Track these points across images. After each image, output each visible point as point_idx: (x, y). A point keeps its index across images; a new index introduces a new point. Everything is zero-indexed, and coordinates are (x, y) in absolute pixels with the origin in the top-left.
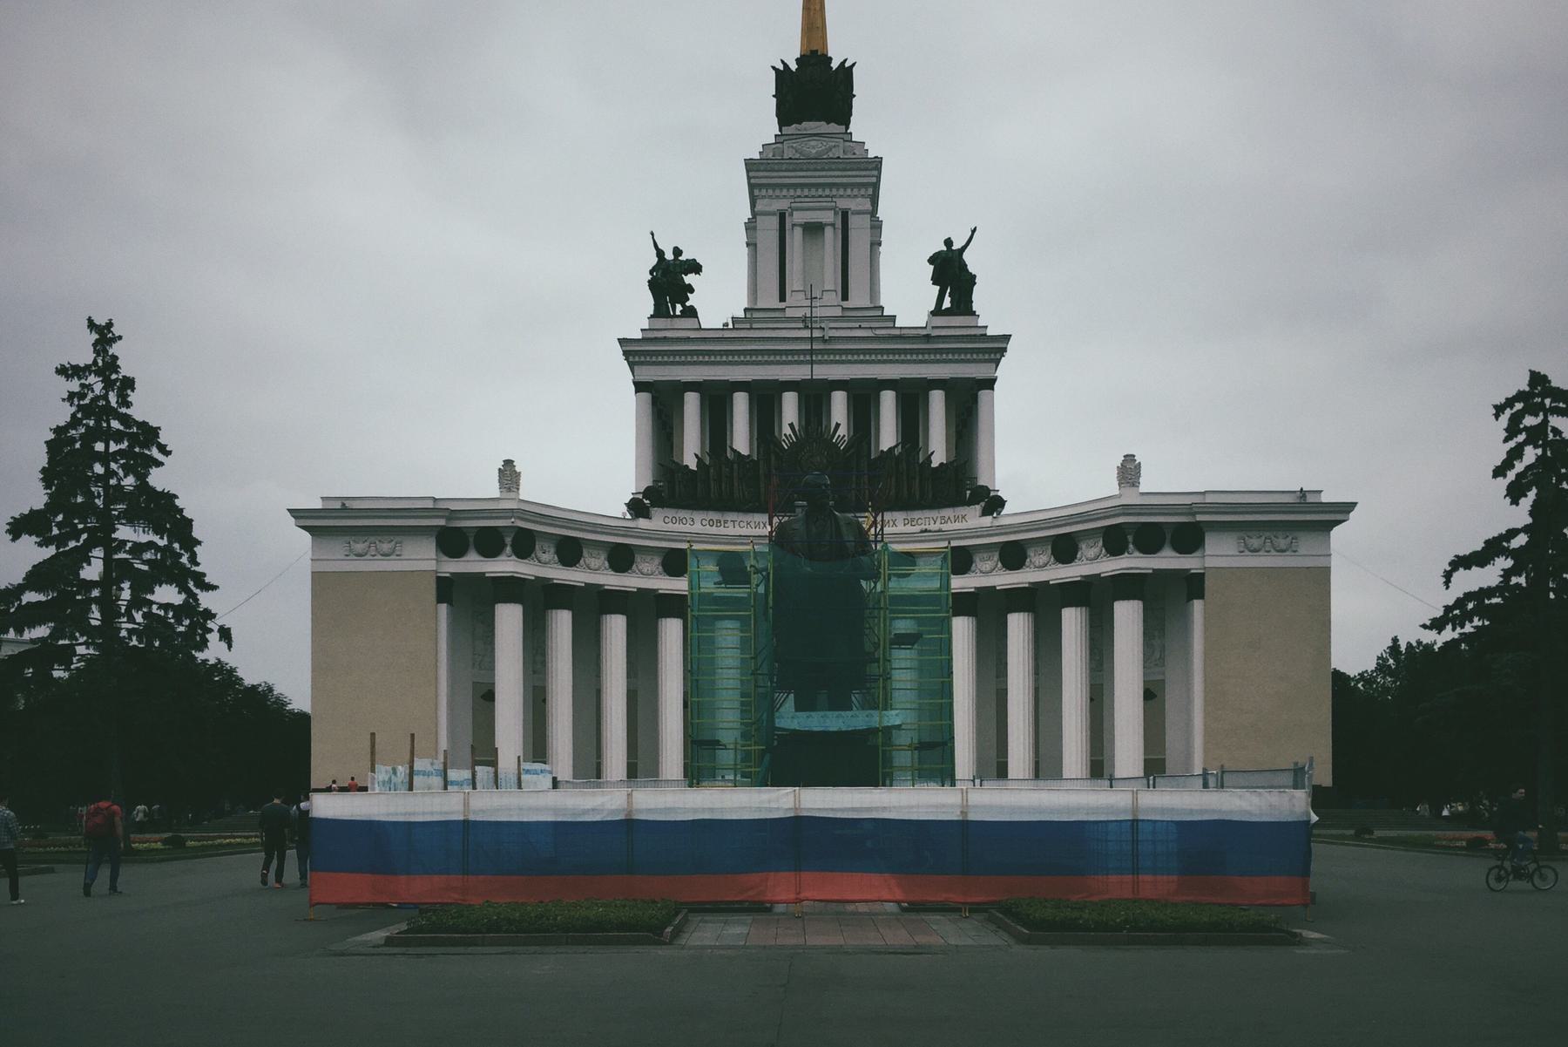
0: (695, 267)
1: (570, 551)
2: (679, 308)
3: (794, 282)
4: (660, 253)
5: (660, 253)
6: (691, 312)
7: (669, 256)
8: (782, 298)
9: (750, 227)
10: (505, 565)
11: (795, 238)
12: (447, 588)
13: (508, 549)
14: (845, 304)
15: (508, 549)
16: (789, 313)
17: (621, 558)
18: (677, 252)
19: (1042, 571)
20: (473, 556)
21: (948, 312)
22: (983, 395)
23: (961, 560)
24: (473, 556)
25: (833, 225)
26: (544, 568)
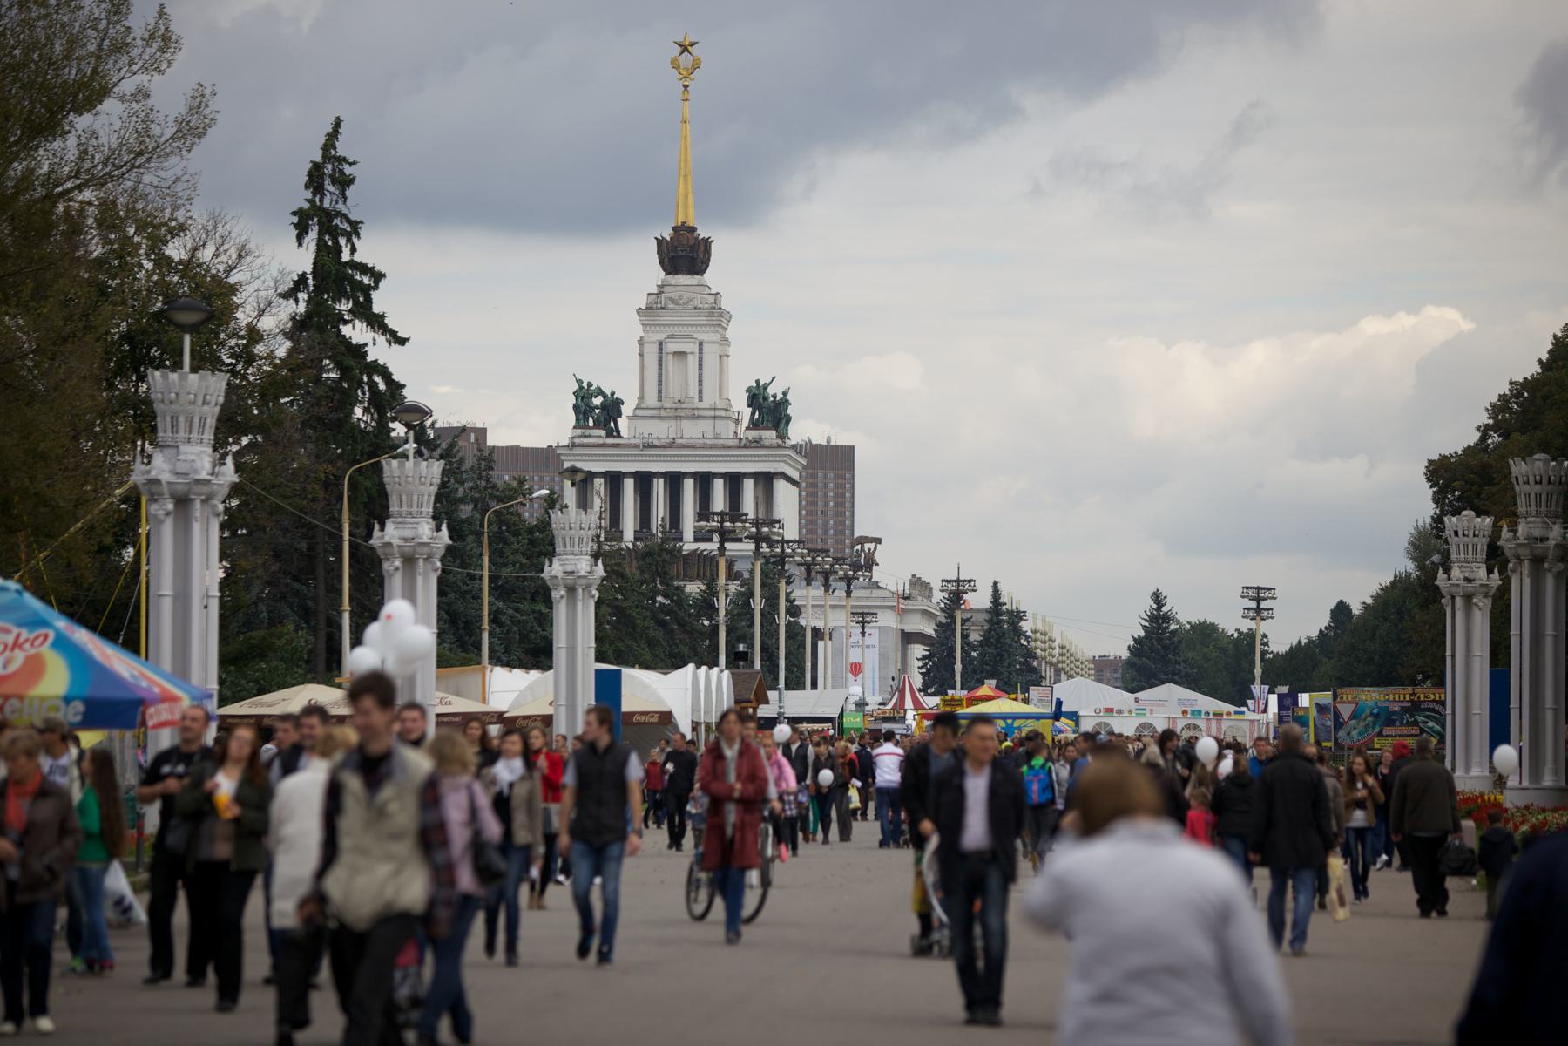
4: (580, 382)
5: (580, 382)
8: (660, 399)
9: (641, 342)
11: (670, 363)
14: (700, 405)
16: (663, 413)
18: (590, 385)
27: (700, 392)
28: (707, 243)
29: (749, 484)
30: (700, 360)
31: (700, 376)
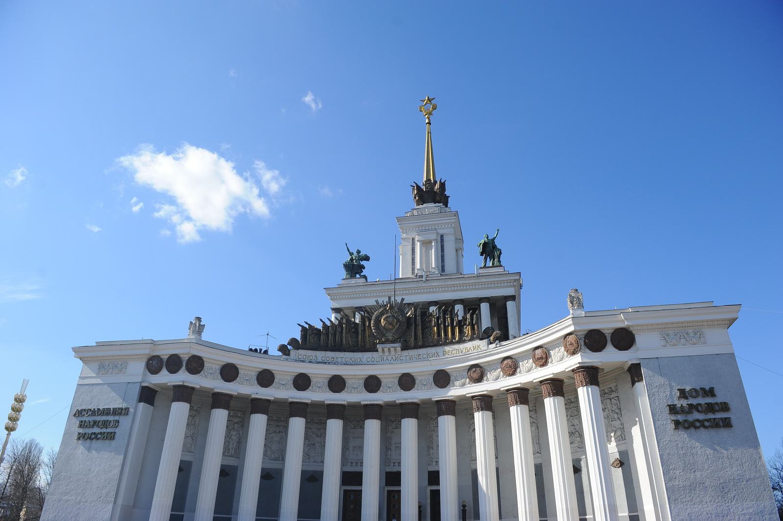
0: (367, 258)
1: (229, 372)
2: (358, 276)
3: (418, 266)
4: (351, 254)
5: (351, 254)
6: (365, 277)
7: (355, 254)
8: (413, 273)
10: (183, 377)
11: (418, 246)
12: (148, 395)
13: (184, 368)
15: (184, 368)
17: (266, 378)
18: (359, 252)
19: (530, 375)
20: (164, 371)
21: (489, 267)
22: (510, 305)
23: (478, 373)
24: (164, 371)
25: (436, 240)
26: (208, 381)
27: (443, 267)
28: (443, 185)
29: (485, 308)
30: (442, 246)
31: (443, 256)
